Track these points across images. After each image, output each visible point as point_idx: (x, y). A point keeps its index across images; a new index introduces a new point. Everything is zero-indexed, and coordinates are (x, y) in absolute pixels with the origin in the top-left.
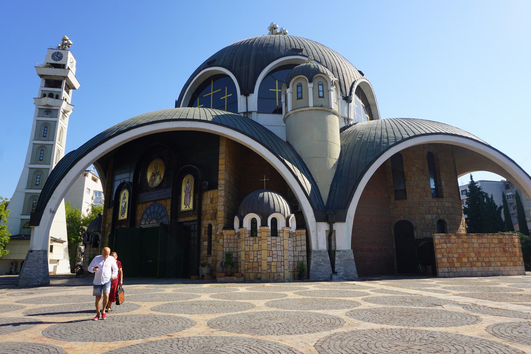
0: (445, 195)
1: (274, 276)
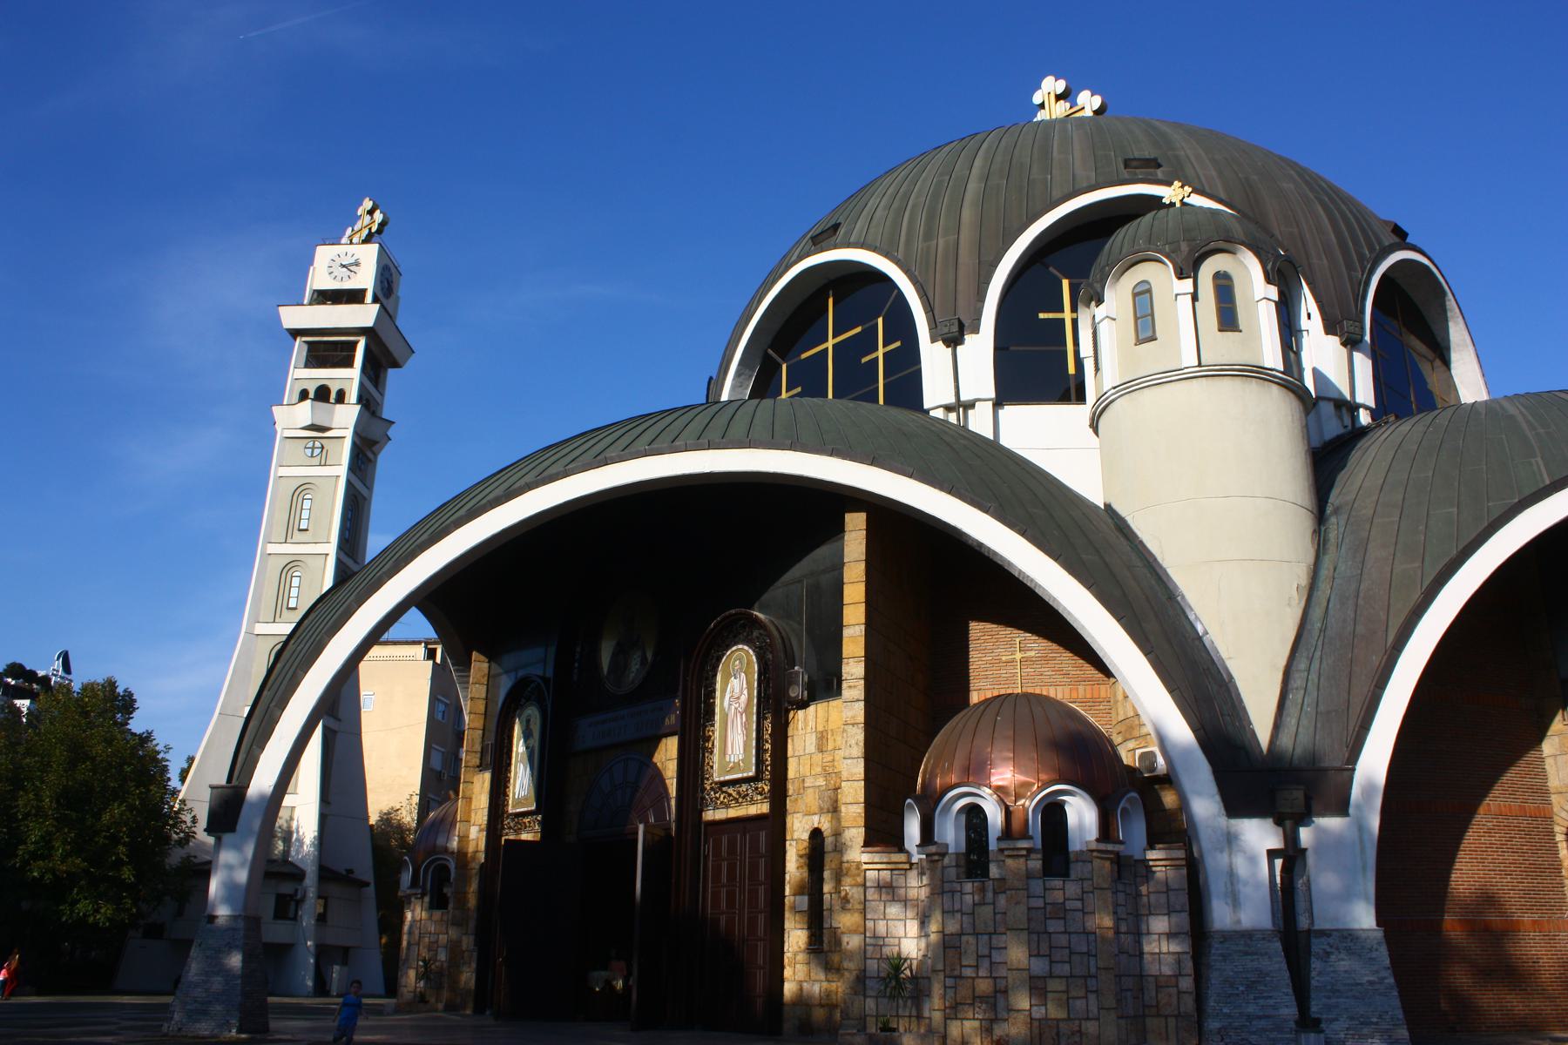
1: (1058, 1034)
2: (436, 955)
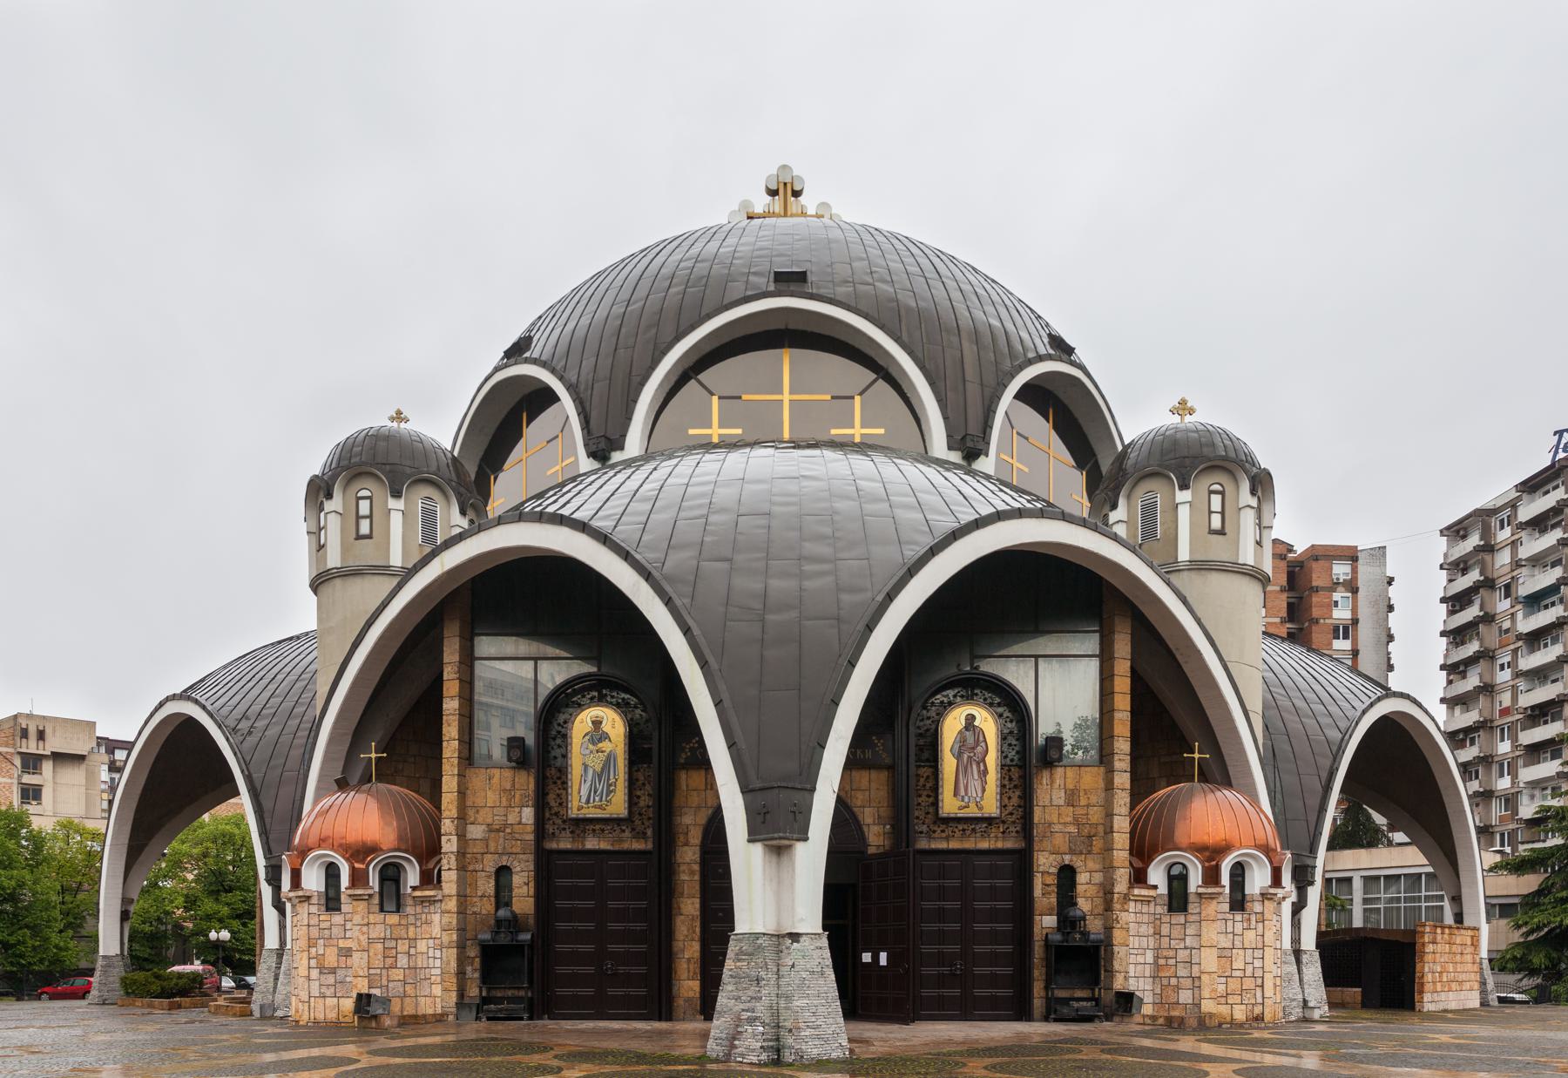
2: (396, 961)
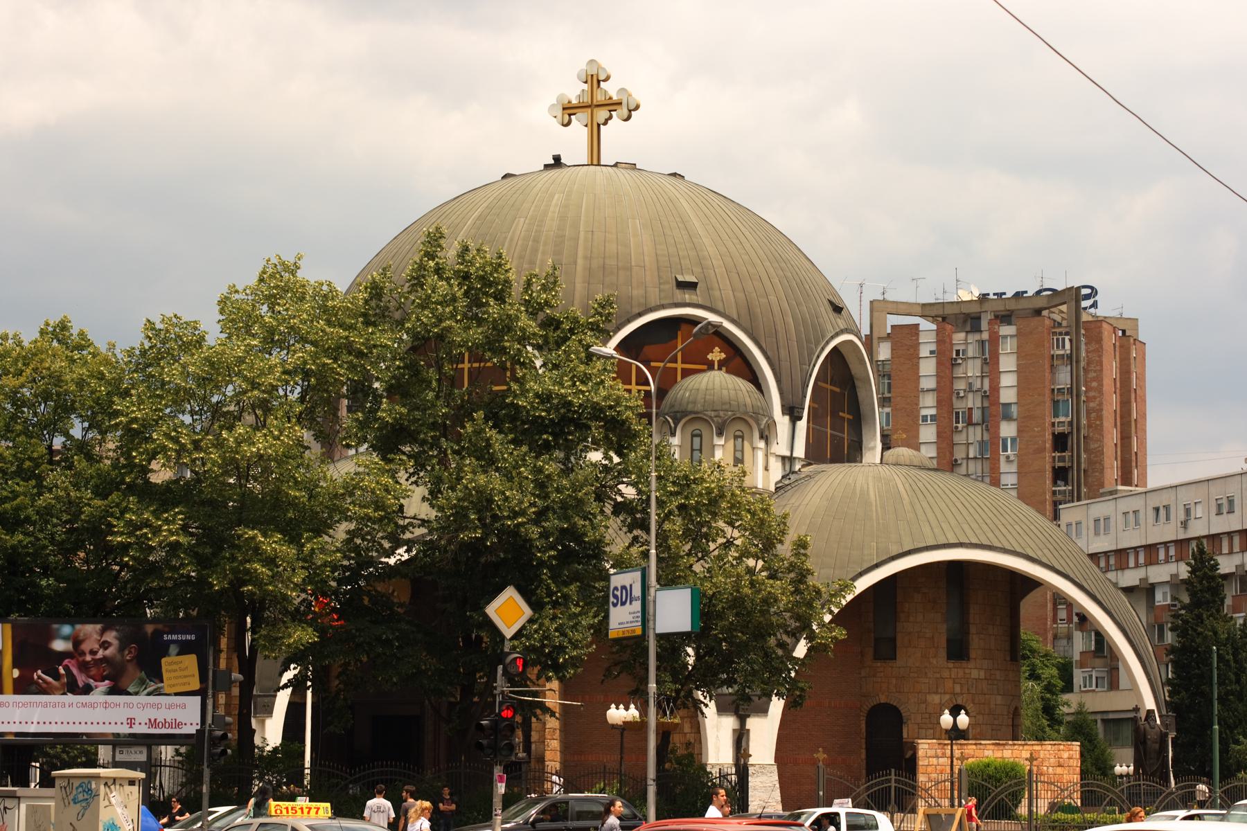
0: (973, 654)
